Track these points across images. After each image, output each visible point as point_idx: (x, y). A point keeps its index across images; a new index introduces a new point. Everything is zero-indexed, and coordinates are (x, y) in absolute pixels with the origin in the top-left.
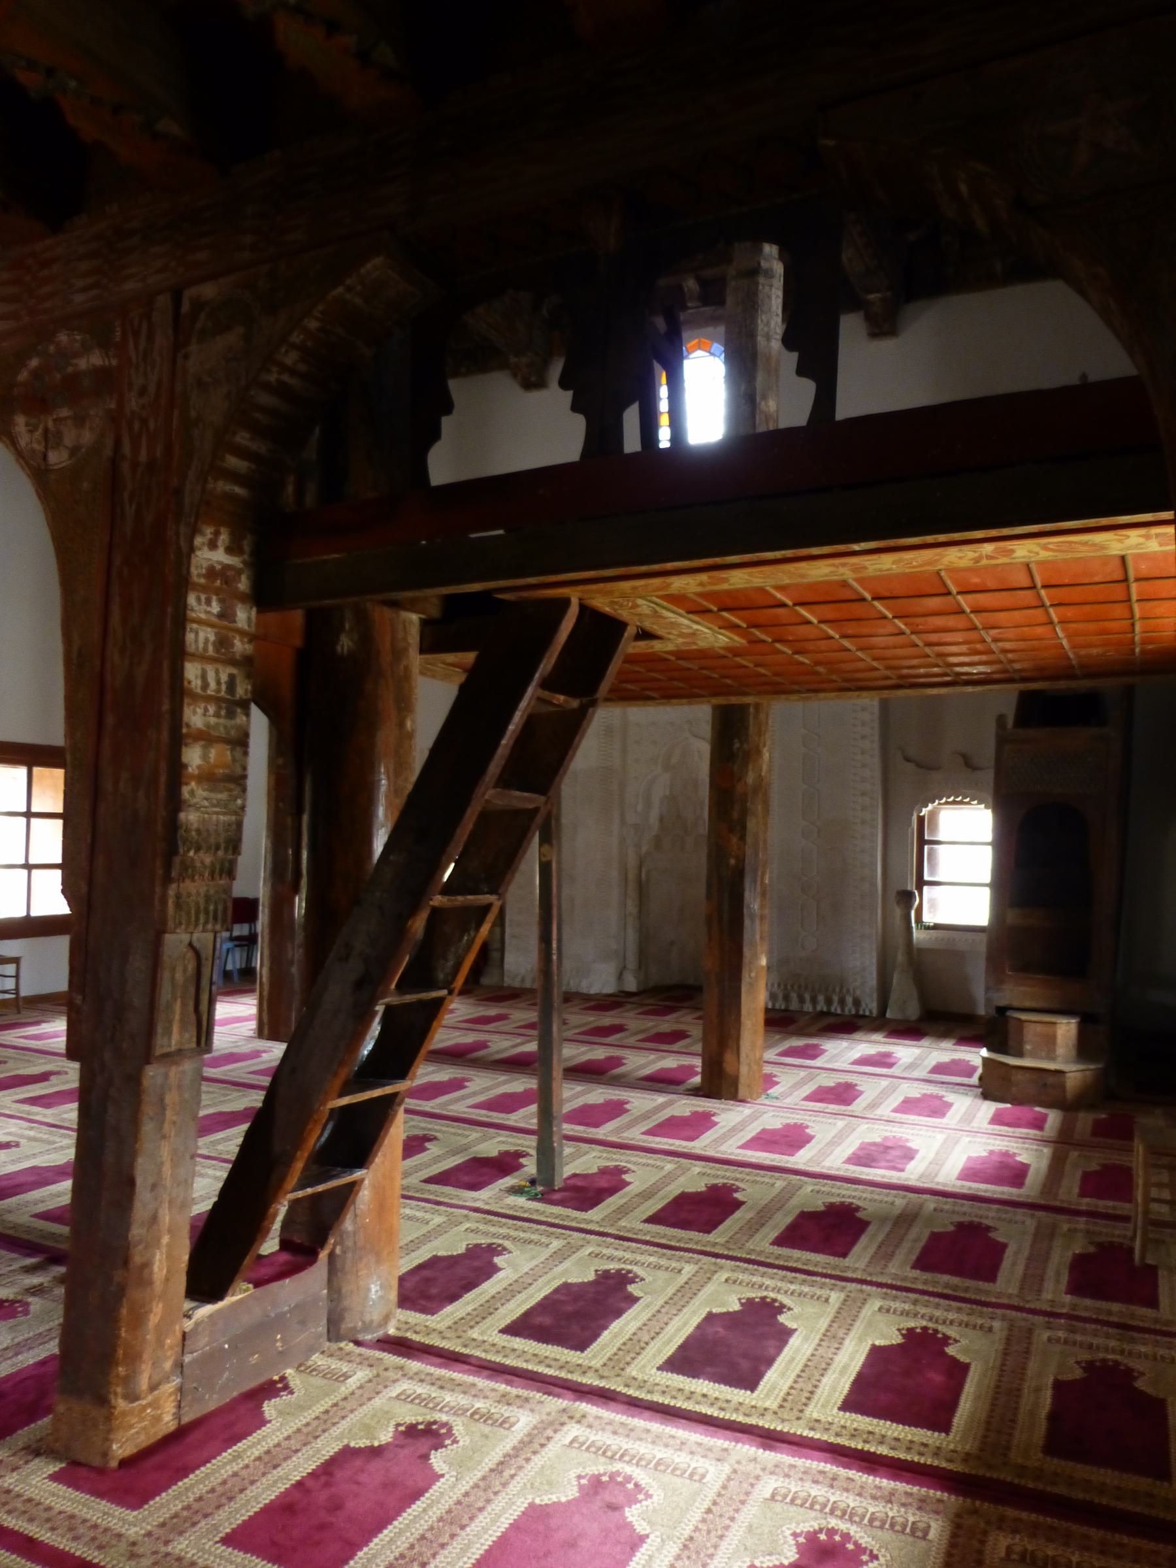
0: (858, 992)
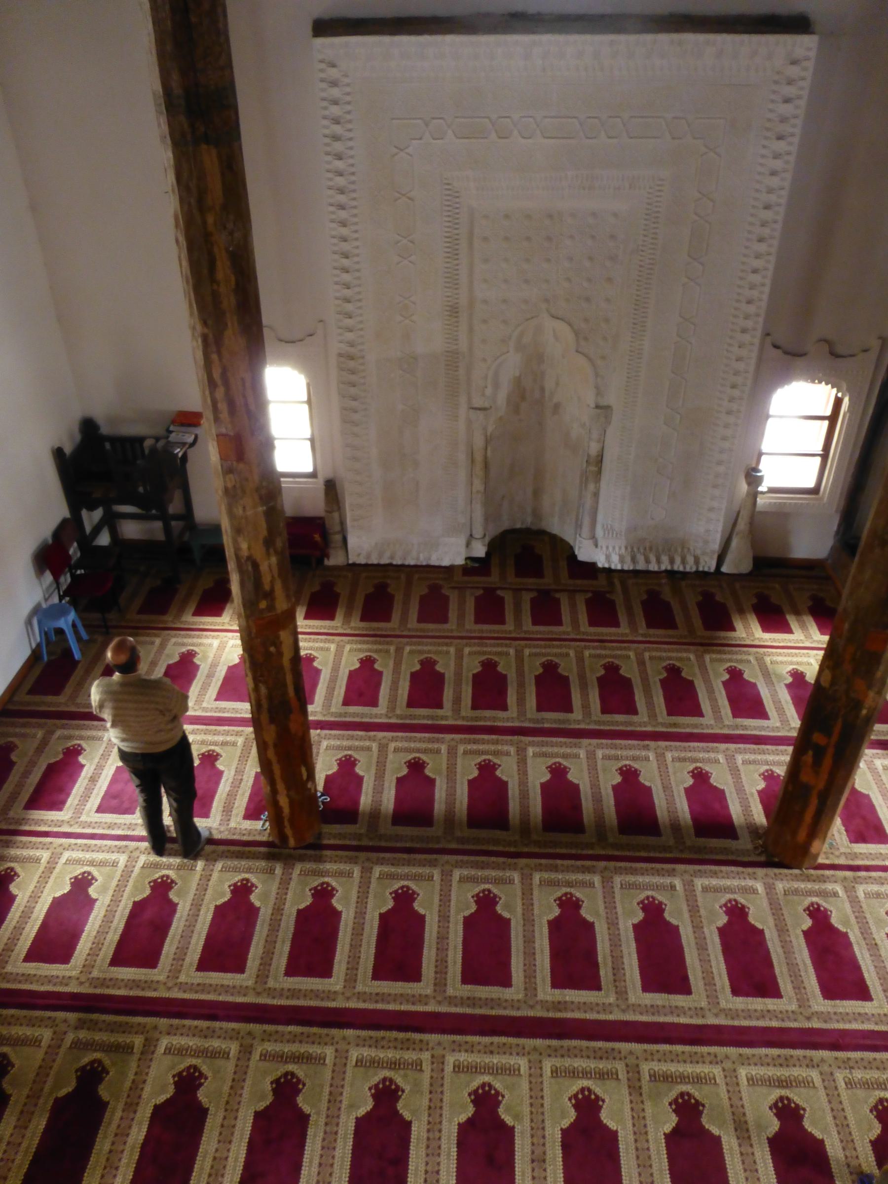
0: (698, 552)
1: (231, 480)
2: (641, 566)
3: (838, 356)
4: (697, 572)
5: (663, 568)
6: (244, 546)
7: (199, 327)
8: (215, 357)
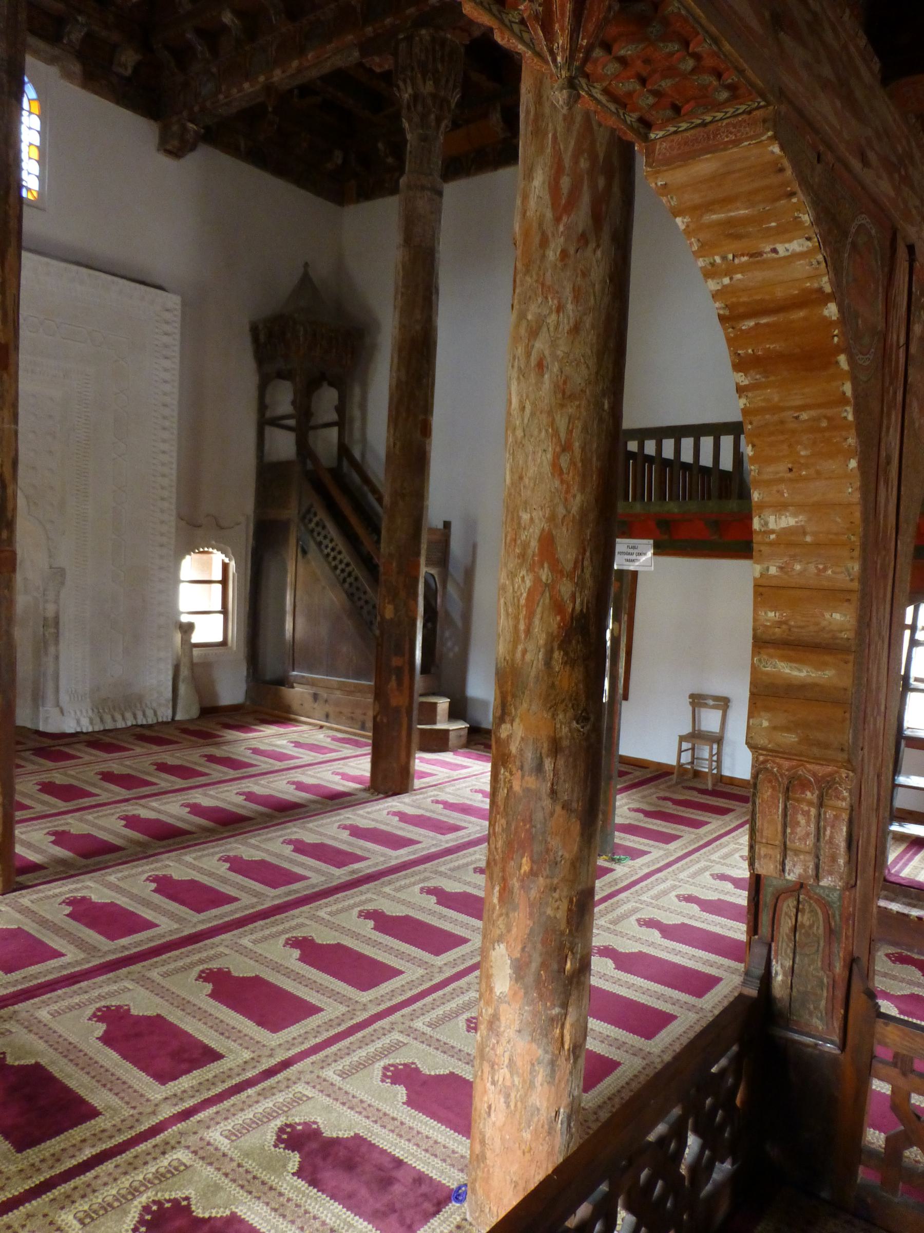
0: (154, 705)
2: (109, 725)
3: (222, 528)
4: (158, 723)
5: (129, 724)
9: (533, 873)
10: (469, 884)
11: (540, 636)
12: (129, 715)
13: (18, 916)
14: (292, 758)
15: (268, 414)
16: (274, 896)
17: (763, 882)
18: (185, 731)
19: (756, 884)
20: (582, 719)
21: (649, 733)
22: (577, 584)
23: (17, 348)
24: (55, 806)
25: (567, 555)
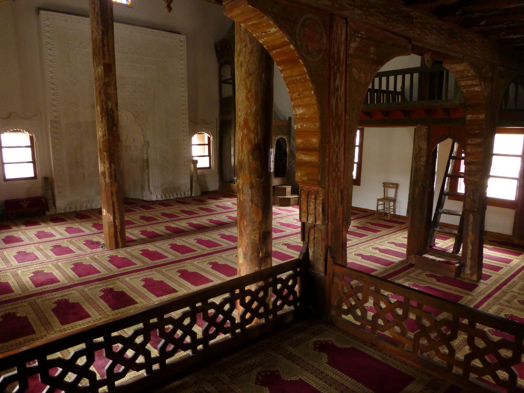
0: (184, 190)
1: (107, 80)
2: (168, 198)
6: (110, 104)
7: (101, 28)
8: (105, 37)
9: (247, 225)
10: (278, 248)
11: (245, 151)
12: (175, 194)
13: (125, 254)
14: (230, 208)
15: (223, 79)
16: (208, 250)
17: (306, 225)
18: (195, 200)
19: (303, 225)
20: (260, 177)
21: (365, 198)
22: (256, 135)
23: (115, 65)
24: (143, 223)
25: (252, 125)
